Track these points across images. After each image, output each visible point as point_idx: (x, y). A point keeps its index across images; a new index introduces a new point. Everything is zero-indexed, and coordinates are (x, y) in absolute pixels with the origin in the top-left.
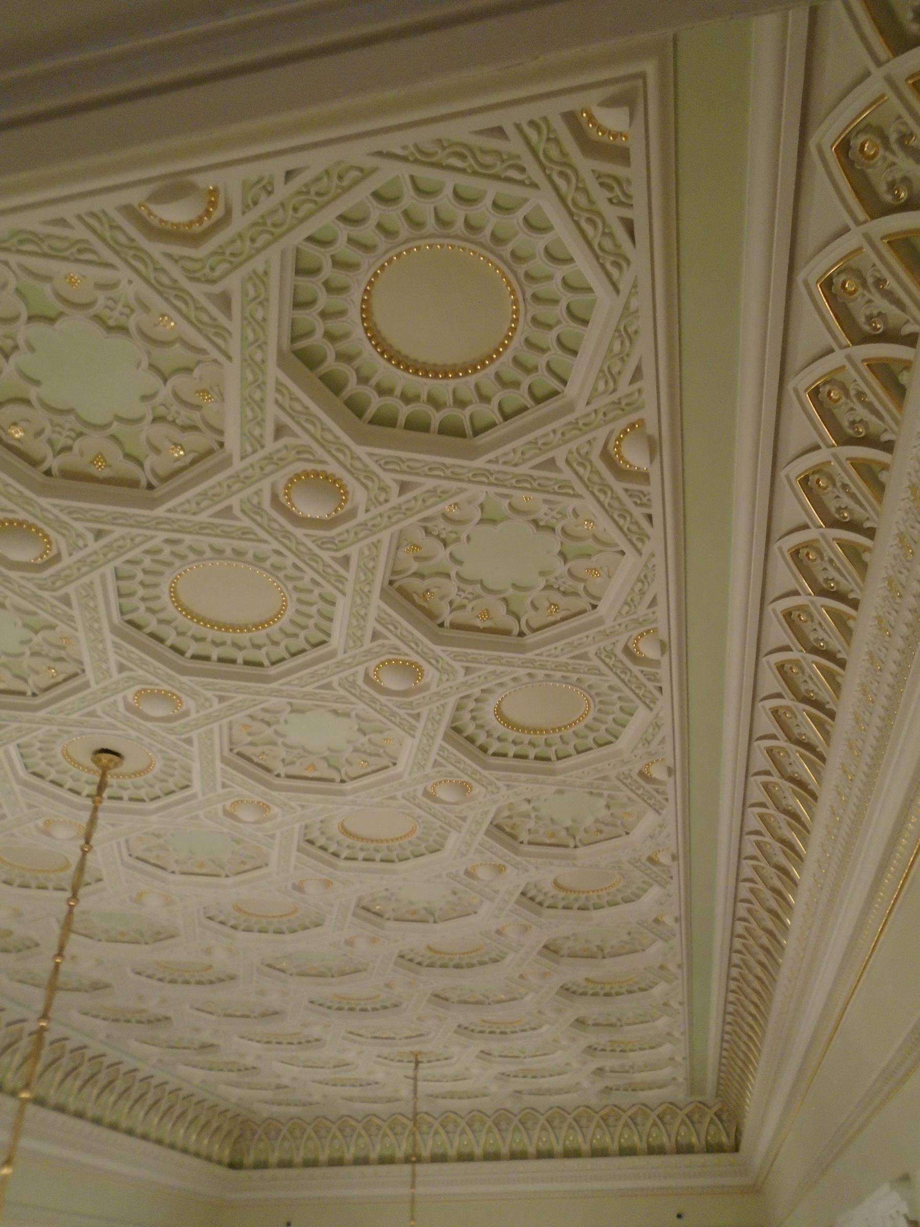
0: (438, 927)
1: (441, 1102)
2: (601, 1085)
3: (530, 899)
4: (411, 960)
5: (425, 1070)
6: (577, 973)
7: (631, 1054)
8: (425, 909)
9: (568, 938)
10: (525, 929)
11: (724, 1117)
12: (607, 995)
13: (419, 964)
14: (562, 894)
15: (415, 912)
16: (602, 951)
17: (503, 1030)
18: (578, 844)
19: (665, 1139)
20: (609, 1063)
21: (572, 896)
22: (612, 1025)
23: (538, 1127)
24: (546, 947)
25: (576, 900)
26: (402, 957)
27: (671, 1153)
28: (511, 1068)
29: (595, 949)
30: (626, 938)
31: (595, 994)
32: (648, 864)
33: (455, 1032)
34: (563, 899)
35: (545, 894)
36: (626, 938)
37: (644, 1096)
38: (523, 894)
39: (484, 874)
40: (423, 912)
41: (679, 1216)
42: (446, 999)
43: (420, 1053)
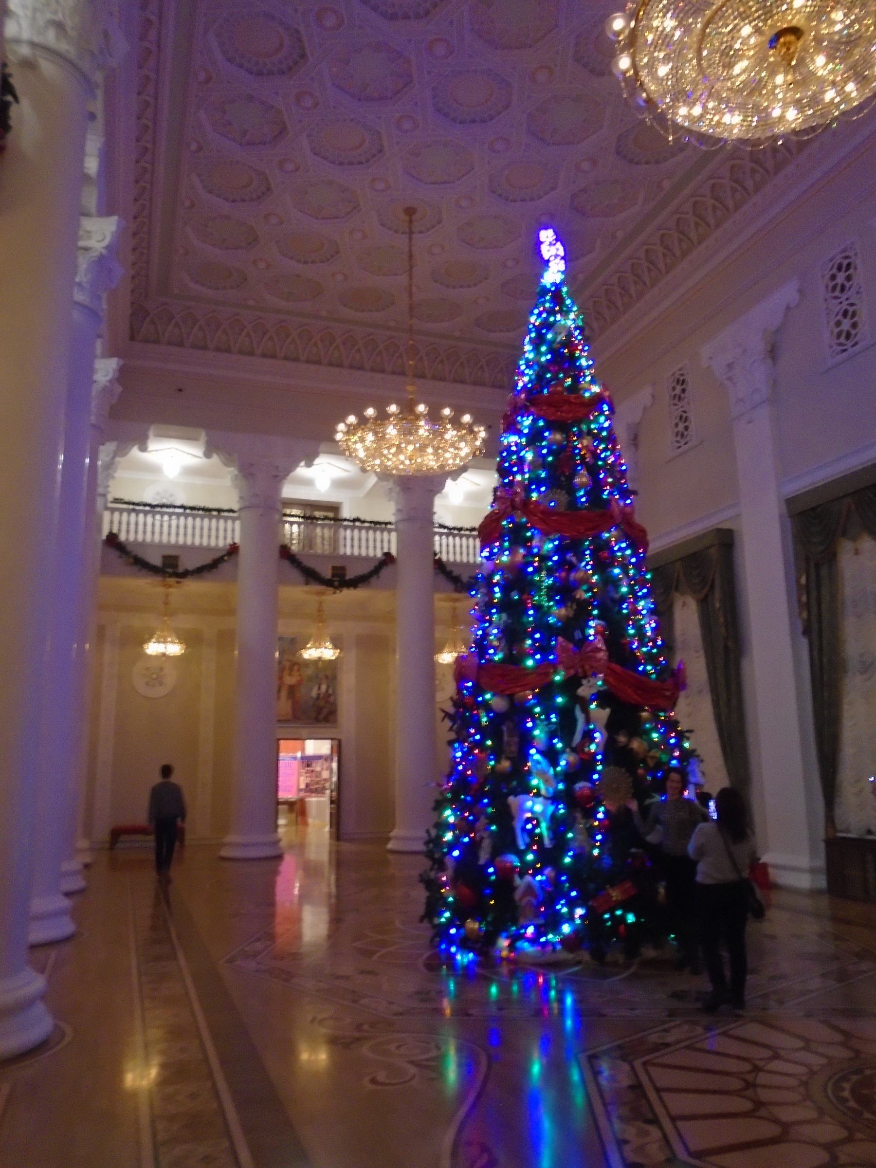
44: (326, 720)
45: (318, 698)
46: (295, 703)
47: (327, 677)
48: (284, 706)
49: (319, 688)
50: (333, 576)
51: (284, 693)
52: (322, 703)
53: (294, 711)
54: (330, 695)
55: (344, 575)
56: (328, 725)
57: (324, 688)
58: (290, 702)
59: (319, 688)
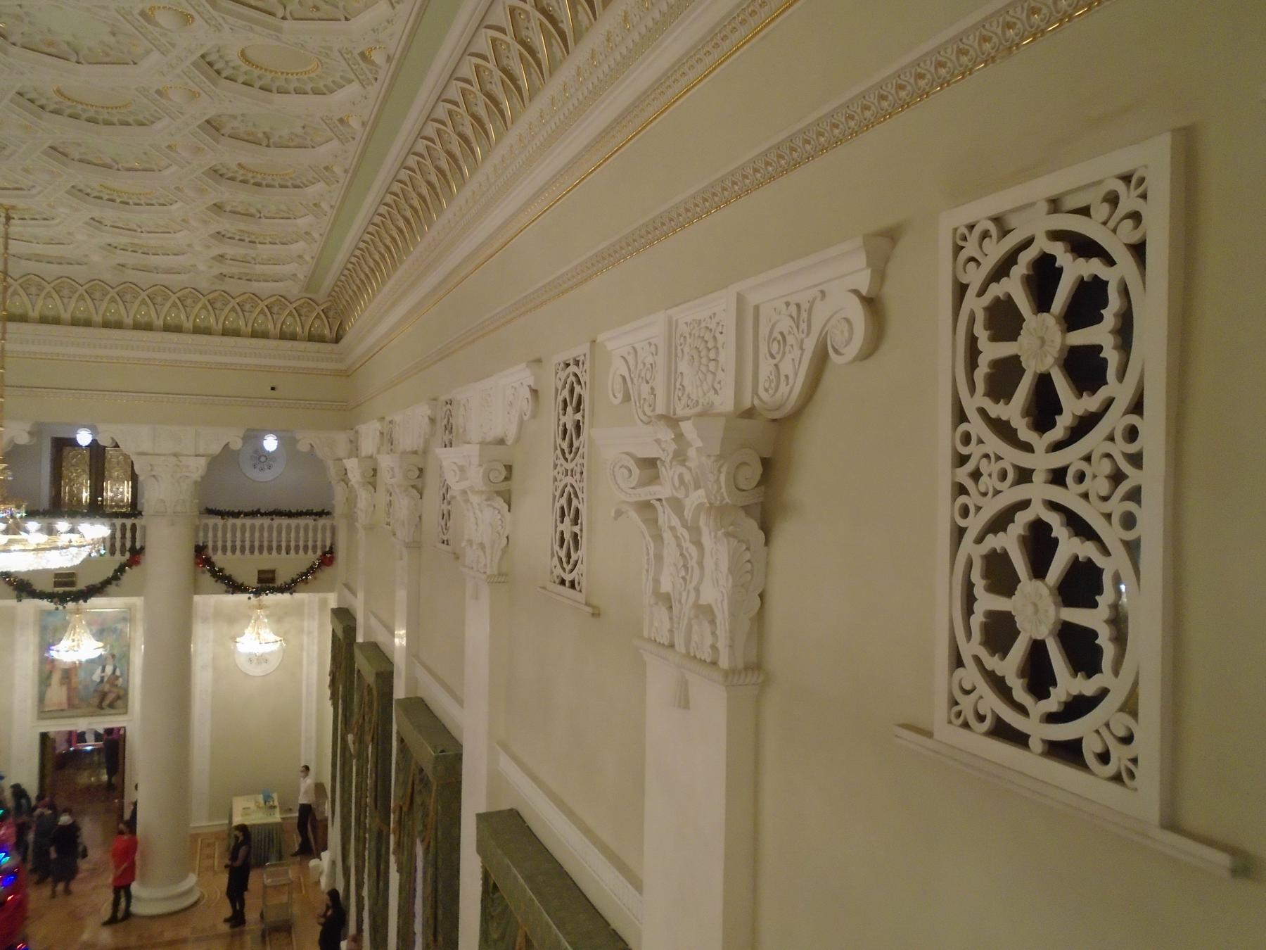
0: (84, 68)
1: (23, 262)
2: (216, 271)
3: (209, 65)
4: (32, 101)
5: (16, 228)
6: (231, 156)
7: (259, 246)
8: (68, 43)
9: (235, 117)
10: (194, 95)
11: (331, 314)
12: (258, 184)
13: (42, 107)
14: (245, 68)
15: (51, 44)
16: (268, 139)
17: (125, 199)
18: (288, 16)
19: (271, 326)
20: (230, 250)
21: (257, 72)
22: (252, 216)
23: (138, 302)
24: (208, 122)
25: (260, 78)
26: (20, 94)
27: (275, 338)
28: (123, 240)
29: (261, 135)
30: (299, 131)
31: (244, 182)
32: (358, 58)
33: (67, 192)
34: (246, 73)
35: (227, 62)
36: (299, 131)
37: (256, 287)
38: (203, 56)
39: (164, 19)
40: (65, 47)
41: (273, 389)
42: (66, 155)
43: (13, 207)
44: (111, 706)
45: (102, 681)
46: (70, 689)
47: (113, 656)
48: (57, 694)
49: (103, 671)
50: (57, 584)
51: (56, 678)
52: (107, 687)
53: (69, 699)
54: (117, 678)
55: (72, 584)
56: (113, 711)
57: (109, 669)
58: (64, 688)
59: (103, 671)
